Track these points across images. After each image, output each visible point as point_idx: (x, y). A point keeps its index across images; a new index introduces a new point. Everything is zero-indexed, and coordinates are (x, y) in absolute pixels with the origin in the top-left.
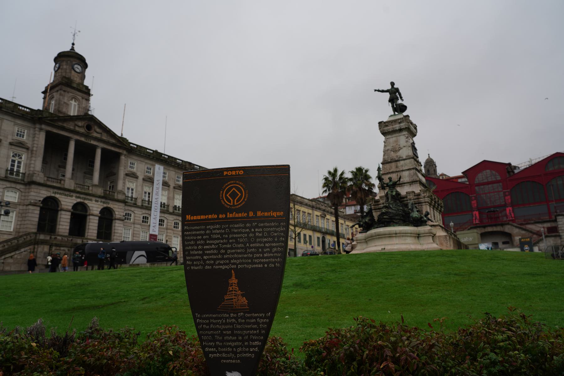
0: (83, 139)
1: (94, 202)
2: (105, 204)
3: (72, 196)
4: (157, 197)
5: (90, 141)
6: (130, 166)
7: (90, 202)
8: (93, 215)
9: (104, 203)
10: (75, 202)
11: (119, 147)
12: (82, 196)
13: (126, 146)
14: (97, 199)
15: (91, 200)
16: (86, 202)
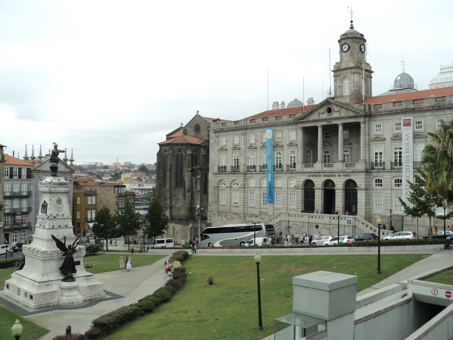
0: (325, 123)
1: (337, 177)
2: (347, 176)
3: (321, 176)
4: (407, 154)
5: (331, 122)
6: (376, 129)
7: (334, 178)
8: (337, 189)
9: (345, 176)
10: (323, 180)
11: (355, 117)
12: (327, 174)
13: (359, 113)
14: (340, 174)
15: (334, 176)
16: (331, 178)
